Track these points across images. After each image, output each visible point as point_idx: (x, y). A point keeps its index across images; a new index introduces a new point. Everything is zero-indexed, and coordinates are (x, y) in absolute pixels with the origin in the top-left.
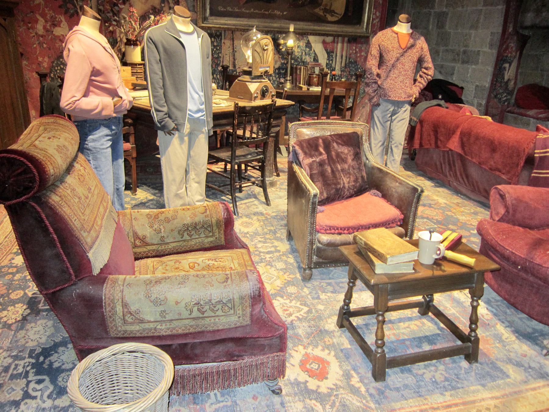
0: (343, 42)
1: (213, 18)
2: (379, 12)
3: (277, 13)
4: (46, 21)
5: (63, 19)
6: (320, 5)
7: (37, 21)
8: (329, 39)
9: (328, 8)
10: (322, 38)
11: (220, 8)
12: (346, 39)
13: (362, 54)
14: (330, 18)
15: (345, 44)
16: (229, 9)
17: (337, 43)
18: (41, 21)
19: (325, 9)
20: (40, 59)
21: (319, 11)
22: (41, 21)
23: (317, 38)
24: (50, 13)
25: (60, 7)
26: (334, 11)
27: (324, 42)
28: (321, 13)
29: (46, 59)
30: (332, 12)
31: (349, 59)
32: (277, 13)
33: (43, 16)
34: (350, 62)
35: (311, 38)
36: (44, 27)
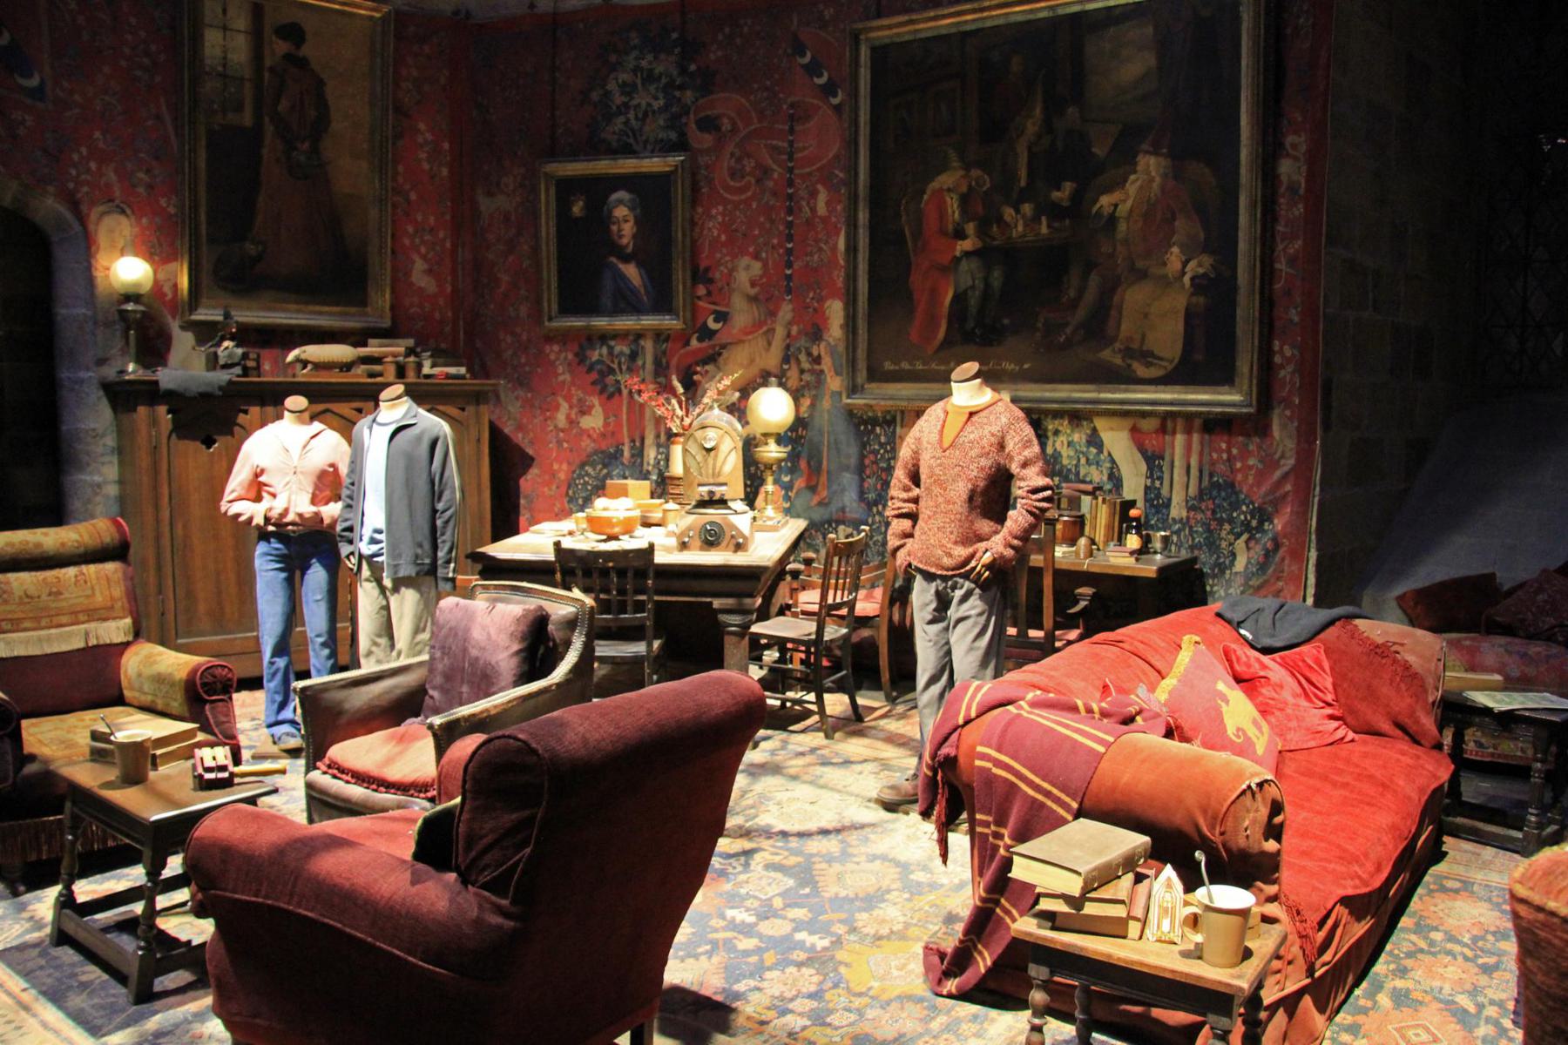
0: (1188, 431)
1: (873, 385)
2: (1293, 347)
3: (1010, 366)
4: (571, 407)
5: (596, 402)
6: (1114, 339)
7: (557, 407)
8: (1148, 425)
9: (1135, 346)
10: (1128, 423)
11: (888, 366)
12: (1198, 422)
13: (1251, 462)
14: (1141, 371)
15: (1196, 437)
16: (905, 365)
17: (1174, 433)
18: (564, 406)
19: (1128, 349)
20: (556, 467)
21: (1111, 356)
22: (564, 406)
23: (1115, 422)
24: (577, 393)
25: (593, 383)
26: (1151, 354)
27: (1134, 430)
28: (1118, 361)
29: (565, 467)
30: (1147, 356)
31: (1211, 475)
32: (1010, 366)
33: (568, 398)
34: (1217, 486)
35: (1100, 423)
36: (568, 417)
